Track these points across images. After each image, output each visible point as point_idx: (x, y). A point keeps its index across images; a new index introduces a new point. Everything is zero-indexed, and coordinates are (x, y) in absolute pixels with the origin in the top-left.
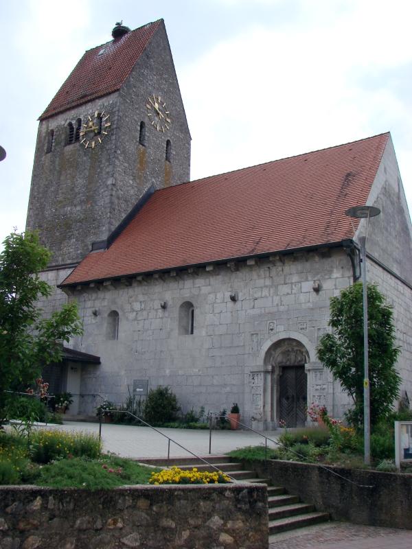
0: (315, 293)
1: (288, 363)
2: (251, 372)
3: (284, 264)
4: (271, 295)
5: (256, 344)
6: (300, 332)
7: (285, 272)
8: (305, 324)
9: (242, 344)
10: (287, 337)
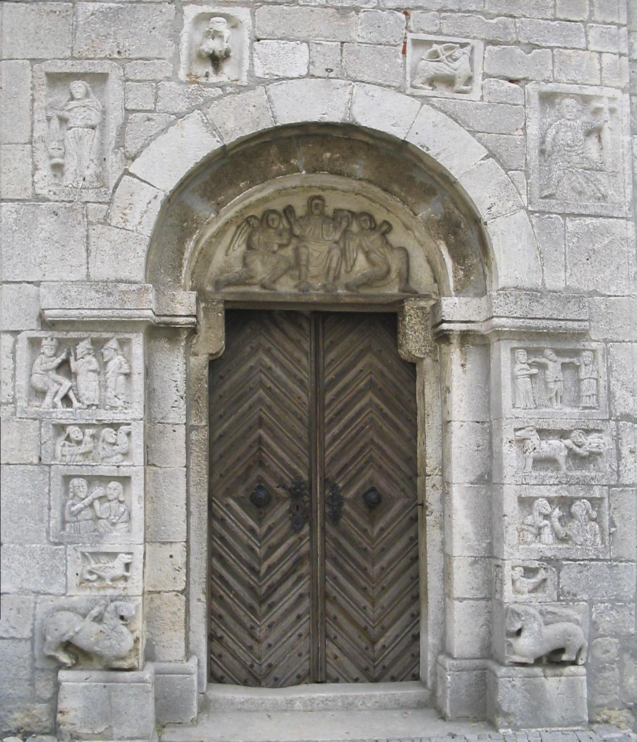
5: (91, 139)
6: (425, 99)
8: (462, 55)
10: (336, 117)
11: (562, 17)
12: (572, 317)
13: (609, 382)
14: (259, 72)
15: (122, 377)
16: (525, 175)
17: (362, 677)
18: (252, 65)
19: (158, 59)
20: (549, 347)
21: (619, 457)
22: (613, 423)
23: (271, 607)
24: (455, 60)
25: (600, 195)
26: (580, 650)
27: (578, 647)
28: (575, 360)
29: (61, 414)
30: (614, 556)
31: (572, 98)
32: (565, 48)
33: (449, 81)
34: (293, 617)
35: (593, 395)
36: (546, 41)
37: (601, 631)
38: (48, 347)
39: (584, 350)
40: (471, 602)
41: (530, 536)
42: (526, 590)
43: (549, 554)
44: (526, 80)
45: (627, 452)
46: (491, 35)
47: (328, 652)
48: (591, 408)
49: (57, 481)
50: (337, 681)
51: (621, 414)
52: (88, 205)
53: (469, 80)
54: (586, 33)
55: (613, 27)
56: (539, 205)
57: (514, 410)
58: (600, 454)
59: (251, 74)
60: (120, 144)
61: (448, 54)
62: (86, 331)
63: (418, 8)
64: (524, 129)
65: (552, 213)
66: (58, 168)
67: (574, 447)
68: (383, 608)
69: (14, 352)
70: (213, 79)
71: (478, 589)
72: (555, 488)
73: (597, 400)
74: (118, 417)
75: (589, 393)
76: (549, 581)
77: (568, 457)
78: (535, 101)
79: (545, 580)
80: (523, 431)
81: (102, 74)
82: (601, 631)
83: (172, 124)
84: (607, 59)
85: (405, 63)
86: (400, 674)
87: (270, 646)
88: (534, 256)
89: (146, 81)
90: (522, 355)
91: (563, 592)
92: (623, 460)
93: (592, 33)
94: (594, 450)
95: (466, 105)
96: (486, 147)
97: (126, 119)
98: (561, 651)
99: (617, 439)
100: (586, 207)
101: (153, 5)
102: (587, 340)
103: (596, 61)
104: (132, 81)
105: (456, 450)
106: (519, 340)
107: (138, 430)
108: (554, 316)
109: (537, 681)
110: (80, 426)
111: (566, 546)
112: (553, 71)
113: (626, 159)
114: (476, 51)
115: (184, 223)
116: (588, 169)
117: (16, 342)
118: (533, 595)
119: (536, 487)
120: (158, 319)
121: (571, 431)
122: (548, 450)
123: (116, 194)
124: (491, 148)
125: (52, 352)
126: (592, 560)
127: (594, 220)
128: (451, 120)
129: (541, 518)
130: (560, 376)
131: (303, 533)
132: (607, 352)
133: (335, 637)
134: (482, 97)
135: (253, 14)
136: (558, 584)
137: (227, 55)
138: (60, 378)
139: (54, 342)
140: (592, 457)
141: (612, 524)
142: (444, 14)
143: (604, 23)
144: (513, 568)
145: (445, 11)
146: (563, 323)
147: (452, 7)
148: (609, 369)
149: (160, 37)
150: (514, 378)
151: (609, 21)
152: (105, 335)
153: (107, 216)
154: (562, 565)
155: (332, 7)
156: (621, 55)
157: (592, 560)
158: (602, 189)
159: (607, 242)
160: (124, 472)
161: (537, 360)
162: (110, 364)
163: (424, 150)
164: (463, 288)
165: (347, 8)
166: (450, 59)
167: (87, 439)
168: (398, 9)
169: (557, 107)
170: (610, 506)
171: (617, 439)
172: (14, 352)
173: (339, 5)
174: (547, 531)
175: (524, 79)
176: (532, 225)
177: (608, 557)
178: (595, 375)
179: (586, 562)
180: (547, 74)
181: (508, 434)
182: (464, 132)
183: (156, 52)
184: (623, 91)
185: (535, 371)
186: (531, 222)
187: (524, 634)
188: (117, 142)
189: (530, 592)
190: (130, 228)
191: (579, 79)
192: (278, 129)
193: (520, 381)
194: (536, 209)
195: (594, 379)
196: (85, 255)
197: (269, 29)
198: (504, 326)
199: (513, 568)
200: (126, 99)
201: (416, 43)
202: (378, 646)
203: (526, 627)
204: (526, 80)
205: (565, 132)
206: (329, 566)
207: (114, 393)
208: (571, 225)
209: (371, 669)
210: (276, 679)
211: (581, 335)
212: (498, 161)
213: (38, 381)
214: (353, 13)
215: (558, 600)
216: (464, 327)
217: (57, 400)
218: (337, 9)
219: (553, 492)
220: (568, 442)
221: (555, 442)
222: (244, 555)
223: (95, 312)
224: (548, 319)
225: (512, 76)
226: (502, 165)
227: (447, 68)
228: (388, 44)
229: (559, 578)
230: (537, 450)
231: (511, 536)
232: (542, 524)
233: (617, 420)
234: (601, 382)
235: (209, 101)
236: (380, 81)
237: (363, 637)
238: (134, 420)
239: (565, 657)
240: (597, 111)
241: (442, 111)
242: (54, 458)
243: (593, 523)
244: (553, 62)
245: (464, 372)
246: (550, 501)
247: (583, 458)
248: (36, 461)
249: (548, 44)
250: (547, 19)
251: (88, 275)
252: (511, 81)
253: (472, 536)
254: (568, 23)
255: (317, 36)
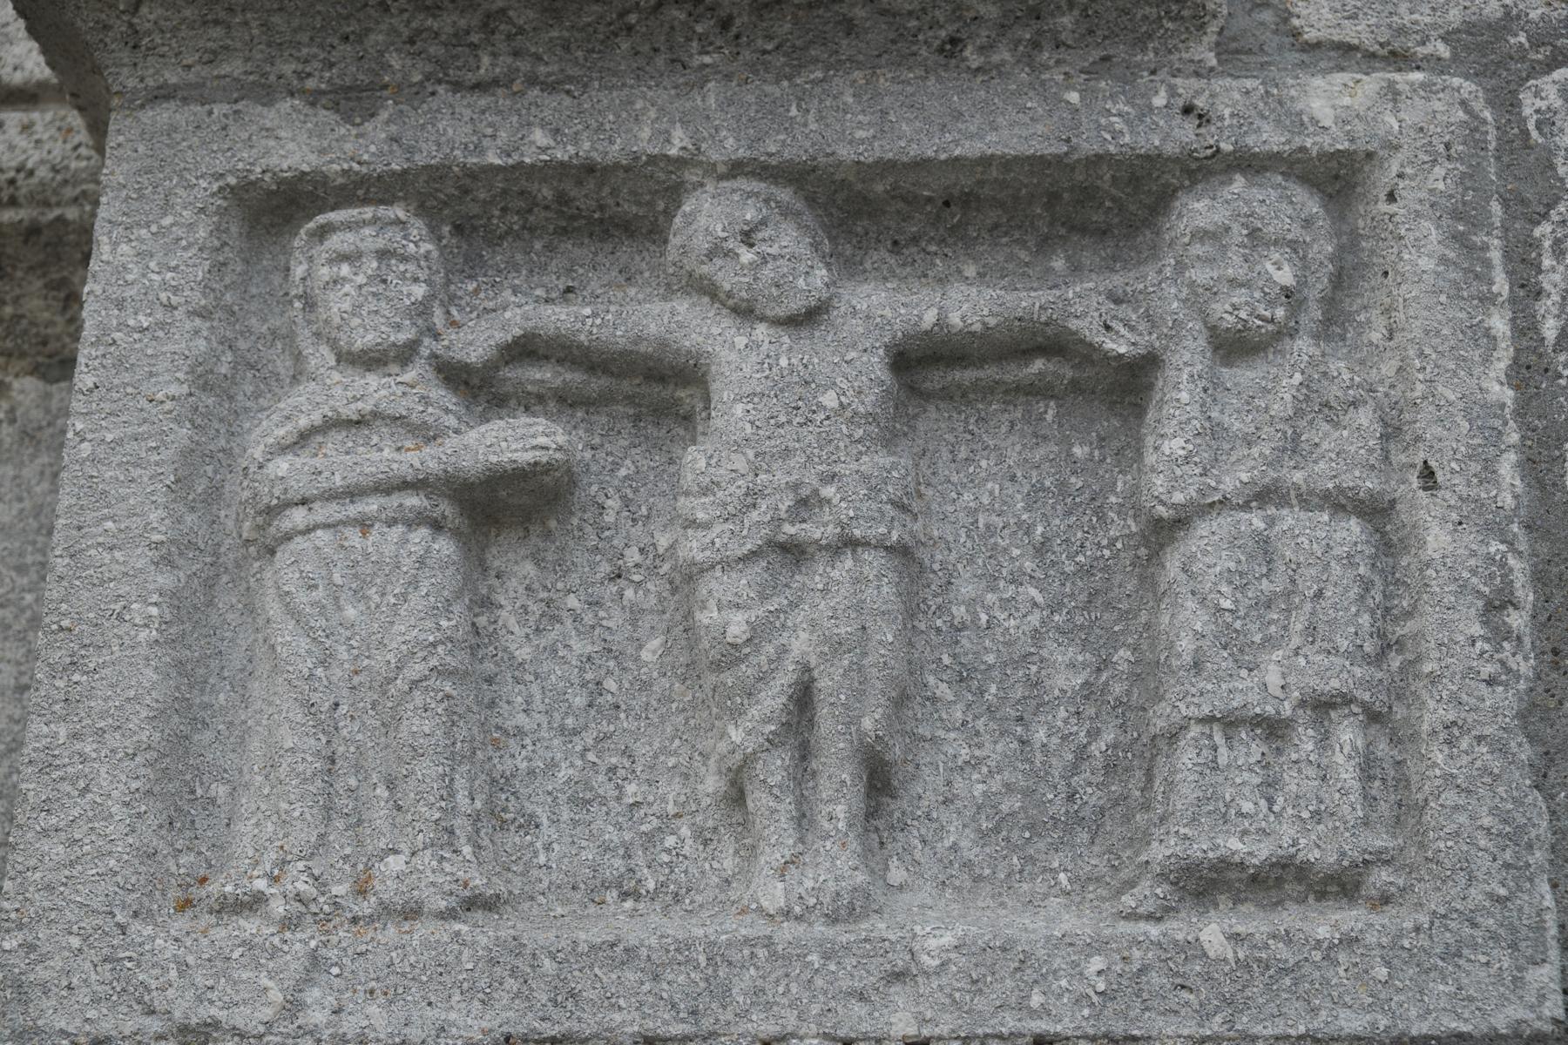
20: (731, 146)
35: (1322, 706)
102: (1233, 53)
161: (558, 318)
195: (1340, 503)
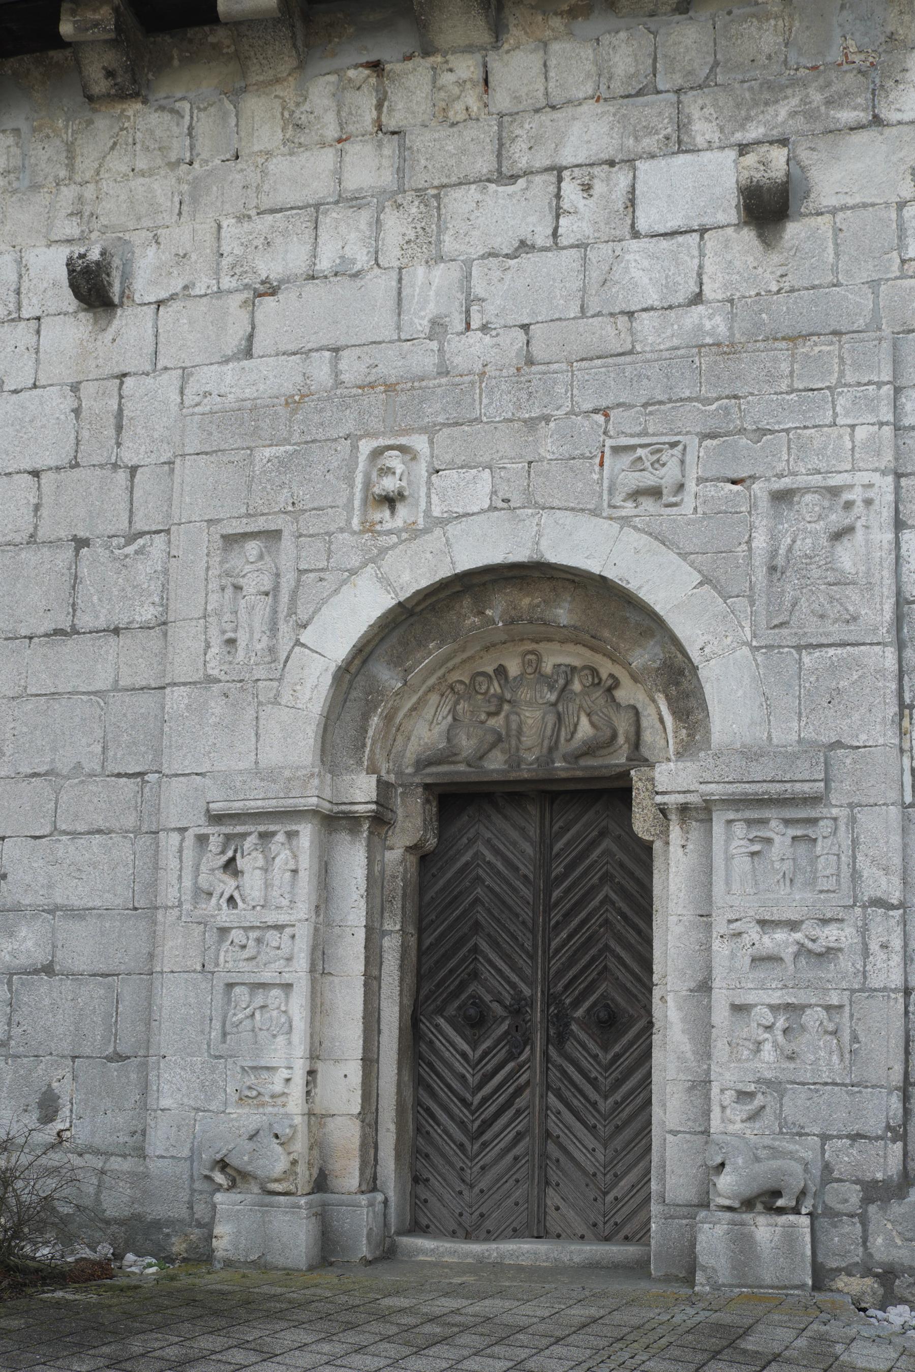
0: (749, 235)
1: (496, 763)
2: (216, 819)
3: (498, 30)
4: (391, 256)
5: (263, 607)
6: (625, 521)
7: (501, 100)
8: (671, 458)
9: (147, 613)
10: (521, 555)
11: (801, 387)
12: (800, 777)
13: (854, 857)
14: (436, 512)
15: (288, 874)
16: (750, 602)
17: (588, 1234)
18: (429, 503)
19: (332, 507)
21: (866, 953)
22: (858, 911)
23: (485, 1145)
24: (664, 465)
25: (848, 617)
26: (803, 1193)
27: (797, 1191)
28: (810, 832)
29: (225, 916)
30: (855, 1080)
31: (816, 492)
32: (806, 427)
33: (655, 493)
34: (509, 1157)
36: (779, 423)
37: (836, 1175)
38: (215, 843)
39: (822, 818)
40: (688, 1136)
41: (746, 1053)
42: (738, 1118)
43: (768, 1075)
44: (753, 478)
45: (877, 948)
46: (712, 425)
47: (549, 1203)
48: (828, 891)
49: (220, 988)
50: (559, 1236)
51: (870, 898)
52: (259, 683)
53: (681, 486)
54: (833, 402)
55: (871, 387)
56: (770, 637)
57: (728, 897)
58: (840, 950)
59: (428, 513)
60: (292, 612)
61: (655, 457)
62: (253, 824)
63: (619, 405)
64: (749, 542)
65: (783, 647)
66: (231, 642)
67: (806, 941)
68: (616, 1151)
69: (180, 851)
70: (387, 526)
71: (695, 1121)
72: (779, 993)
73: (838, 881)
74: (283, 919)
75: (828, 872)
76: (768, 1109)
77: (797, 956)
78: (764, 503)
79: (763, 1107)
80: (738, 923)
81: (276, 531)
82: (836, 1175)
83: (344, 582)
84: (861, 433)
85: (602, 479)
86: (636, 1233)
87: (482, 1191)
88: (758, 703)
89: (318, 534)
90: (739, 829)
91: (786, 1123)
92: (871, 957)
93: (841, 401)
94: (832, 945)
95: (675, 521)
96: (699, 572)
97: (299, 581)
98: (777, 1194)
99: (864, 931)
100: (827, 635)
101: (328, 443)
103: (847, 438)
104: (305, 536)
105: (672, 950)
106: (737, 811)
107: (304, 933)
108: (777, 778)
109: (746, 1230)
110: (246, 929)
111: (792, 1066)
112: (788, 461)
113: (885, 565)
114: (688, 449)
115: (368, 694)
116: (834, 584)
117: (183, 840)
118: (747, 1125)
119: (753, 992)
120: (336, 809)
121: (802, 922)
122: (771, 945)
123: (286, 669)
124: (706, 573)
125: (219, 849)
126: (826, 1084)
127: (839, 651)
128: (657, 543)
129: (761, 1031)
130: (789, 852)
131: (523, 1058)
132: (853, 820)
133: (558, 1185)
134: (695, 509)
135: (431, 442)
136: (781, 1114)
137: (401, 496)
138: (225, 878)
139: (221, 839)
140: (829, 954)
141: (855, 1039)
142: (650, 408)
143: (859, 384)
144: (722, 1091)
145: (652, 405)
146: (788, 785)
147: (660, 398)
148: (855, 842)
149: (334, 482)
150: (729, 858)
151: (866, 380)
152: (272, 828)
153: (278, 695)
154: (785, 1089)
155: (519, 419)
156: (881, 424)
157: (826, 1084)
158: (851, 609)
159: (856, 677)
160: (287, 978)
161: (759, 834)
162: (277, 860)
163: (624, 584)
164: (685, 750)
165: (537, 418)
166: (657, 466)
167: (251, 943)
168: (596, 411)
169: (796, 507)
170: (852, 1016)
171: (864, 931)
172: (180, 851)
173: (527, 416)
174: (768, 1046)
175: (750, 477)
176: (757, 665)
177: (848, 1081)
178: (835, 849)
179: (817, 1087)
180: (781, 466)
181: (720, 926)
182: (673, 556)
183: (330, 499)
184: (884, 473)
185: (756, 847)
186: (755, 660)
187: (728, 1169)
188: (289, 609)
189: (742, 1121)
190: (300, 706)
191: (823, 466)
192: (457, 576)
193: (736, 862)
194: (763, 644)
196: (254, 740)
197: (448, 457)
198: (712, 794)
199: (722, 1091)
200: (298, 558)
201: (616, 450)
202: (610, 1198)
203: (727, 1162)
204: (753, 478)
205: (804, 539)
206: (552, 1099)
207: (279, 892)
208: (807, 659)
209: (601, 1225)
210: (488, 1232)
211: (814, 800)
212: (715, 587)
213: (204, 880)
214: (543, 423)
215: (781, 1133)
216: (681, 799)
217: (223, 901)
218: (525, 421)
219: (776, 998)
220: (798, 936)
221: (781, 935)
222: (456, 1085)
223: (259, 803)
224: (770, 781)
225: (735, 476)
226: (719, 593)
227: (652, 477)
228: (582, 456)
229: (781, 1107)
230: (757, 946)
231: (720, 1049)
232: (761, 1038)
233: (864, 907)
234: (843, 858)
235: (383, 551)
236: (572, 505)
237: (592, 1186)
238: (300, 921)
239: (780, 1203)
240: (849, 505)
241: (646, 533)
242: (217, 965)
243: (828, 1038)
244: (789, 448)
245: (685, 854)
246: (774, 1008)
247: (820, 955)
248: (199, 968)
249: (782, 427)
250: (782, 393)
251: (257, 763)
252: (734, 482)
253: (689, 1055)
254: (810, 393)
255: (501, 458)
